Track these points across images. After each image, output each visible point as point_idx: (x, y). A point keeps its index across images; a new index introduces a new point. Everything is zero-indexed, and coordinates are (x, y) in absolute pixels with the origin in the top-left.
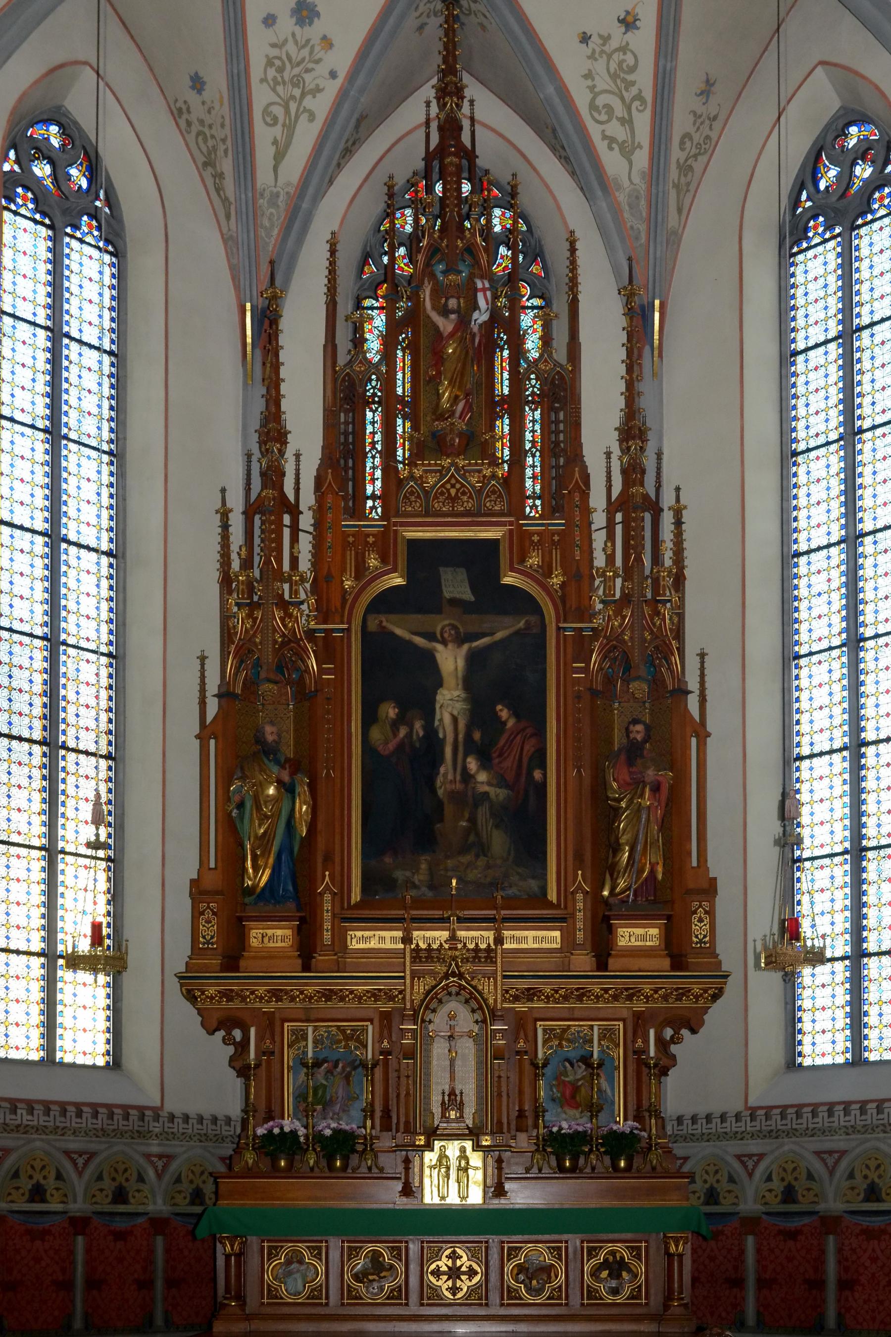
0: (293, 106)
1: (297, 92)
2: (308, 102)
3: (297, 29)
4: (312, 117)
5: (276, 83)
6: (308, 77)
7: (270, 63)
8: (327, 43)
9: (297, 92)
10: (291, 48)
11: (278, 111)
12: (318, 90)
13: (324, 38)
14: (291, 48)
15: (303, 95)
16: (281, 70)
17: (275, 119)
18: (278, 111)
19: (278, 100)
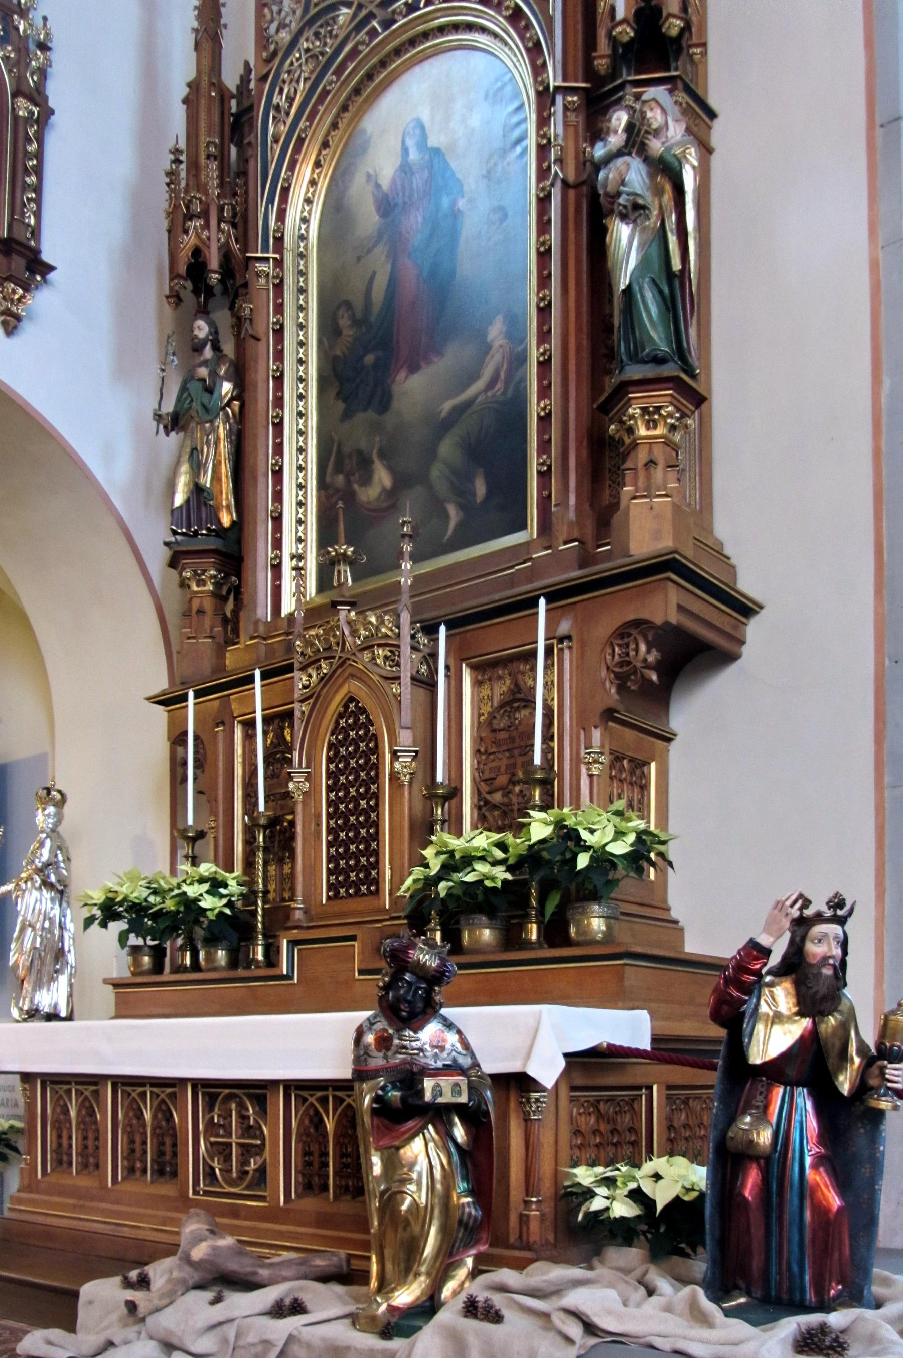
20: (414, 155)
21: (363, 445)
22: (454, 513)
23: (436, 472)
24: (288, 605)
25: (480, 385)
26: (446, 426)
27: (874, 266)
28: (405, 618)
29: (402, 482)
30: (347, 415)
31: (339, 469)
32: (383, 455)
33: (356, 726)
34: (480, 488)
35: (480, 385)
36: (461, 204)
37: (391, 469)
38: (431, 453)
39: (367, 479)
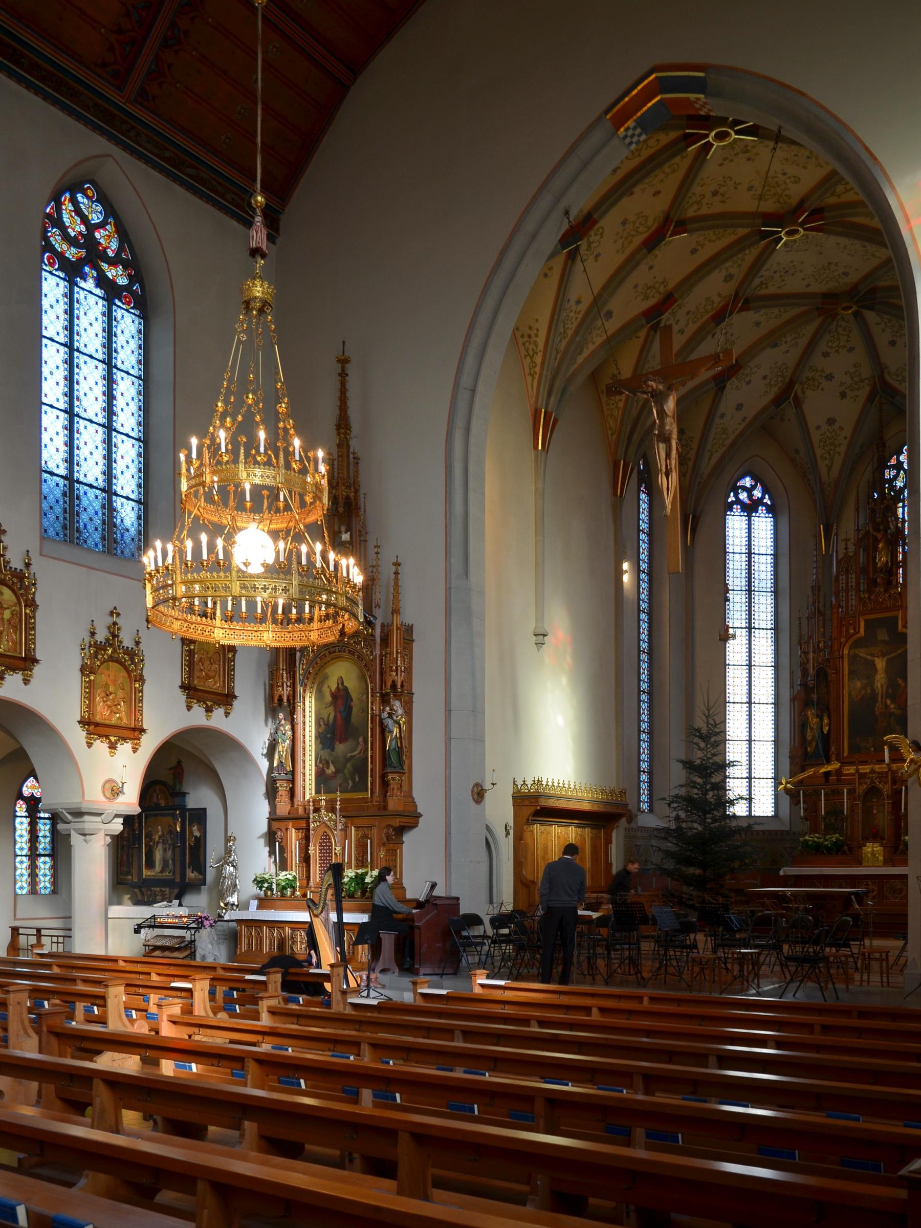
0: (832, 452)
1: (833, 447)
2: (837, 449)
3: (829, 427)
4: (840, 454)
5: (824, 446)
6: (835, 442)
7: (820, 441)
8: (841, 428)
9: (833, 447)
10: (828, 434)
11: (827, 455)
12: (841, 444)
13: (840, 427)
14: (828, 434)
15: (835, 447)
16: (825, 442)
17: (826, 458)
18: (827, 455)
19: (824, 451)
20: (340, 686)
21: (327, 758)
22: (351, 784)
23: (346, 771)
24: (307, 797)
25: (356, 753)
26: (349, 760)
27: (446, 742)
28: (338, 815)
29: (337, 771)
30: (323, 749)
31: (321, 762)
32: (332, 763)
33: (326, 839)
34: (357, 779)
35: (356, 753)
36: (352, 704)
37: (335, 767)
38: (345, 767)
39: (328, 768)
